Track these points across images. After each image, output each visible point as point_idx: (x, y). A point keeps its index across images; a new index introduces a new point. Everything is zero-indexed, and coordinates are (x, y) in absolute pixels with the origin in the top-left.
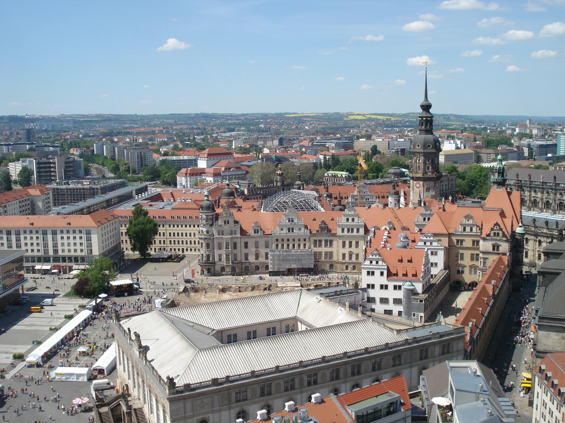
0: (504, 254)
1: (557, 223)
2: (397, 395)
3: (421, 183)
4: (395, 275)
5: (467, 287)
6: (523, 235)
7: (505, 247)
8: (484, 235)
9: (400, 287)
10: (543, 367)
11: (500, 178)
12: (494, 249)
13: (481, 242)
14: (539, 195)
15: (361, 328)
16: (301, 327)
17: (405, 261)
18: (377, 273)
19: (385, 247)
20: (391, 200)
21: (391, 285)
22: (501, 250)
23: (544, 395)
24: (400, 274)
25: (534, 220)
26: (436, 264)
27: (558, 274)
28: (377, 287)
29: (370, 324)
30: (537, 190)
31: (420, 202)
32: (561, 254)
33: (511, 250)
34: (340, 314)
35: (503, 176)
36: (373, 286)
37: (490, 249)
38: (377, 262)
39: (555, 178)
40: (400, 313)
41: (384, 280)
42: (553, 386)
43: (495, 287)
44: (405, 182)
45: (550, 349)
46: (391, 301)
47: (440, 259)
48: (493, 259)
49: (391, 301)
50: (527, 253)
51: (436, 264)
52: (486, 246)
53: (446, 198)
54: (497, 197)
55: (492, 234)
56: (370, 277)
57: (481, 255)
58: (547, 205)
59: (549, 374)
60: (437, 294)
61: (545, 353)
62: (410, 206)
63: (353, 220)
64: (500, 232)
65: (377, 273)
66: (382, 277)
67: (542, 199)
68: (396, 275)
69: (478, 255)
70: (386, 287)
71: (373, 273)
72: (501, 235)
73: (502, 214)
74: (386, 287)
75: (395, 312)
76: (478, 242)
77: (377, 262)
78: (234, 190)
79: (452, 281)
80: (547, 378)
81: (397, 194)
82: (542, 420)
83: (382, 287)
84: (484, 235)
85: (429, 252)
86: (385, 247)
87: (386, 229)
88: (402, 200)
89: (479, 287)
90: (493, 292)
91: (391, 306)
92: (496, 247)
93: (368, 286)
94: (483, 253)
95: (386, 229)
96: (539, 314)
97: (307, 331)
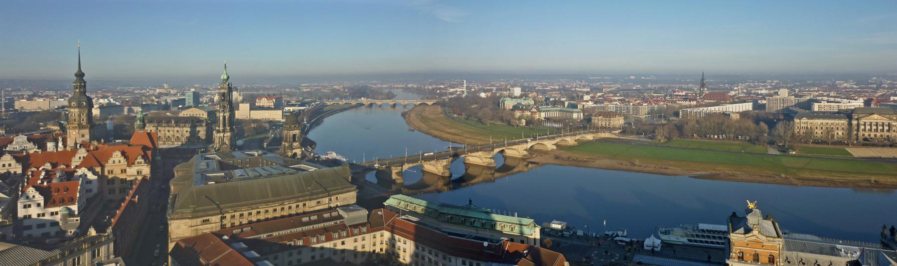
7: (146, 170)
13: (128, 169)
19: (42, 182)
20: (50, 146)
22: (144, 173)
26: (91, 190)
30: (170, 129)
31: (76, 144)
51: (91, 190)
62: (68, 149)
64: (143, 161)
76: (125, 171)
81: (56, 141)
86: (42, 182)
88: (60, 144)
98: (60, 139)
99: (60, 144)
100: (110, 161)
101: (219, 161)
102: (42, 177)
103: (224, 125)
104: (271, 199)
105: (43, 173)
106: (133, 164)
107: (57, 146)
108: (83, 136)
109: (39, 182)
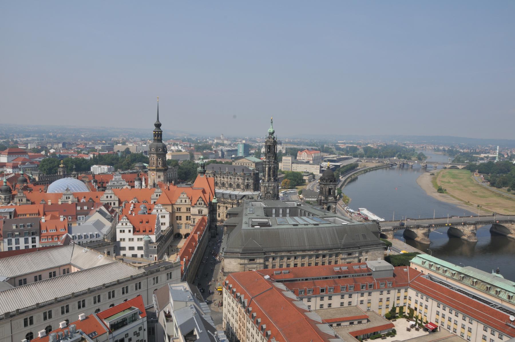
0: (205, 215)
1: (236, 196)
2: (137, 309)
3: (155, 173)
4: (138, 231)
5: (183, 237)
6: (216, 203)
7: (205, 211)
8: (193, 204)
9: (141, 239)
10: (227, 282)
11: (202, 169)
12: (199, 213)
13: (192, 209)
14: (226, 179)
15: (114, 267)
16: (74, 270)
17: (144, 222)
18: (127, 231)
19: (132, 214)
20: (137, 183)
21: (136, 237)
22: (203, 213)
23: (229, 298)
24: (141, 231)
25: (223, 194)
26: (164, 223)
27: (235, 226)
28: (127, 240)
29: (121, 264)
30: (224, 176)
31: (154, 184)
32: (237, 214)
33: (209, 213)
34: (101, 259)
35: (204, 168)
36: (124, 239)
37: (197, 213)
38: (126, 224)
39: (234, 169)
40: (142, 256)
41: (131, 235)
42: (233, 292)
43: (200, 236)
44: (146, 171)
45: (232, 271)
46: (136, 248)
47: (167, 220)
48: (198, 218)
49: (136, 248)
50: (219, 214)
51: (164, 223)
52: (194, 211)
53: (170, 182)
54: (200, 181)
55: (198, 204)
56: (122, 234)
57: (192, 217)
58: (231, 185)
59: (231, 286)
60: (166, 242)
61: (228, 273)
62: (149, 187)
63: (111, 197)
64: (203, 202)
65: (127, 231)
66: (130, 234)
67: (227, 182)
68: (139, 231)
69: (190, 217)
70: (133, 239)
71: (124, 231)
72: (203, 204)
73: (204, 192)
74: (133, 239)
75: (139, 256)
76: (190, 209)
77: (126, 224)
78: (27, 178)
79: (175, 233)
80: (230, 288)
81: (140, 180)
82: (228, 313)
83: (130, 239)
84: (193, 204)
85: (160, 216)
87: (132, 202)
88: (143, 183)
89: (190, 237)
90: (199, 239)
91: (136, 252)
92: (200, 212)
93: (121, 239)
94: (193, 215)
95: (132, 202)
96: (225, 250)
97: (78, 272)
98: (143, 180)
99: (143, 183)
100: (179, 201)
101: (264, 208)
102: (131, 209)
103: (269, 175)
104: (307, 248)
105: (132, 205)
106: (196, 204)
107: (141, 184)
108: (159, 177)
109: (130, 213)
